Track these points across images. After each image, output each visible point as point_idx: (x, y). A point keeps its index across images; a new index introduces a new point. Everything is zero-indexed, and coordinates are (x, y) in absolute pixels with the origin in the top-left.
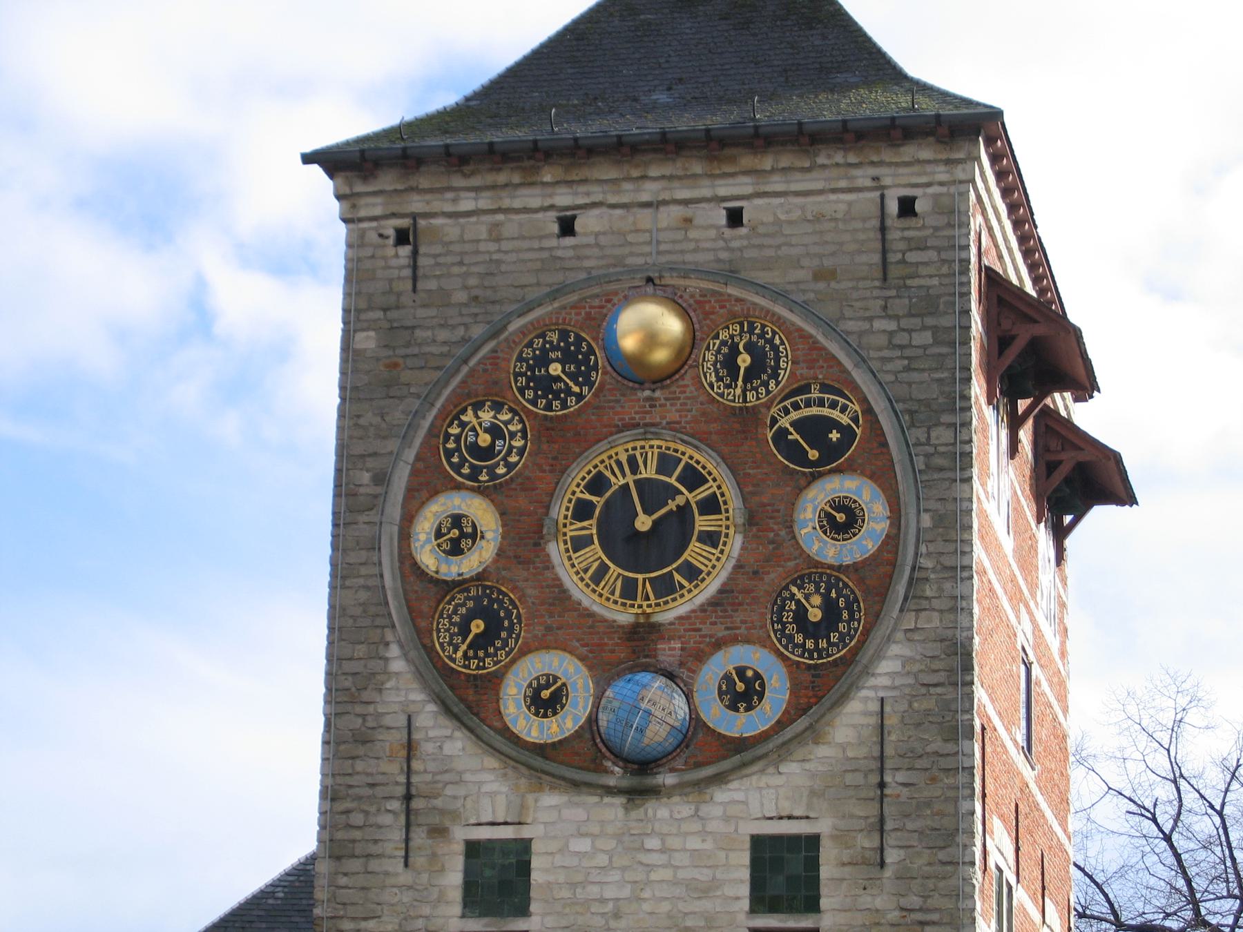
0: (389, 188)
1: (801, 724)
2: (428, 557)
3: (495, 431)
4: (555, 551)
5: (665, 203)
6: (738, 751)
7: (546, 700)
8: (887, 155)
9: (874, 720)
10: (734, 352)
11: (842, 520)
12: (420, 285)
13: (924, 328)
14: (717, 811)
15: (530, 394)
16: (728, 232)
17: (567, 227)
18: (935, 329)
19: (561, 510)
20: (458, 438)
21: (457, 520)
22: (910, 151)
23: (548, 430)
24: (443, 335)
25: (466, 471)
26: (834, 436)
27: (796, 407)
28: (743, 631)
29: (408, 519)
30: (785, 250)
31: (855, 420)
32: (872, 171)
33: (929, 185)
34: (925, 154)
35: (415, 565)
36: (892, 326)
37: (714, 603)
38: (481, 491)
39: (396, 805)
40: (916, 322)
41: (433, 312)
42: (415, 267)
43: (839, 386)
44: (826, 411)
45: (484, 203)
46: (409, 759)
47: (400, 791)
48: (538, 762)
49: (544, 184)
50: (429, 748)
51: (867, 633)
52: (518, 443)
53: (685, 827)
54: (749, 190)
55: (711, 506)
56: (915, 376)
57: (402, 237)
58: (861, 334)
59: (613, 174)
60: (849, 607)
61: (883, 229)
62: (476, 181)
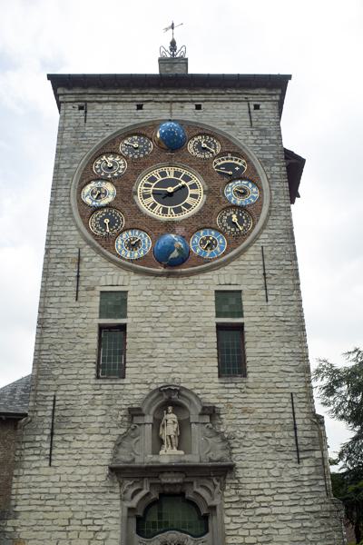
0: (78, 92)
2: (88, 200)
4: (139, 199)
7: (133, 246)
8: (251, 92)
10: (200, 143)
11: (242, 193)
17: (140, 107)
18: (270, 139)
20: (100, 165)
26: (237, 168)
28: (208, 225)
34: (264, 91)
35: (85, 204)
37: (195, 216)
40: (263, 138)
43: (238, 154)
44: (233, 161)
45: (110, 99)
46: (79, 263)
51: (254, 226)
52: (122, 167)
55: (194, 186)
57: (81, 108)
58: (245, 140)
60: (246, 219)
61: (250, 112)
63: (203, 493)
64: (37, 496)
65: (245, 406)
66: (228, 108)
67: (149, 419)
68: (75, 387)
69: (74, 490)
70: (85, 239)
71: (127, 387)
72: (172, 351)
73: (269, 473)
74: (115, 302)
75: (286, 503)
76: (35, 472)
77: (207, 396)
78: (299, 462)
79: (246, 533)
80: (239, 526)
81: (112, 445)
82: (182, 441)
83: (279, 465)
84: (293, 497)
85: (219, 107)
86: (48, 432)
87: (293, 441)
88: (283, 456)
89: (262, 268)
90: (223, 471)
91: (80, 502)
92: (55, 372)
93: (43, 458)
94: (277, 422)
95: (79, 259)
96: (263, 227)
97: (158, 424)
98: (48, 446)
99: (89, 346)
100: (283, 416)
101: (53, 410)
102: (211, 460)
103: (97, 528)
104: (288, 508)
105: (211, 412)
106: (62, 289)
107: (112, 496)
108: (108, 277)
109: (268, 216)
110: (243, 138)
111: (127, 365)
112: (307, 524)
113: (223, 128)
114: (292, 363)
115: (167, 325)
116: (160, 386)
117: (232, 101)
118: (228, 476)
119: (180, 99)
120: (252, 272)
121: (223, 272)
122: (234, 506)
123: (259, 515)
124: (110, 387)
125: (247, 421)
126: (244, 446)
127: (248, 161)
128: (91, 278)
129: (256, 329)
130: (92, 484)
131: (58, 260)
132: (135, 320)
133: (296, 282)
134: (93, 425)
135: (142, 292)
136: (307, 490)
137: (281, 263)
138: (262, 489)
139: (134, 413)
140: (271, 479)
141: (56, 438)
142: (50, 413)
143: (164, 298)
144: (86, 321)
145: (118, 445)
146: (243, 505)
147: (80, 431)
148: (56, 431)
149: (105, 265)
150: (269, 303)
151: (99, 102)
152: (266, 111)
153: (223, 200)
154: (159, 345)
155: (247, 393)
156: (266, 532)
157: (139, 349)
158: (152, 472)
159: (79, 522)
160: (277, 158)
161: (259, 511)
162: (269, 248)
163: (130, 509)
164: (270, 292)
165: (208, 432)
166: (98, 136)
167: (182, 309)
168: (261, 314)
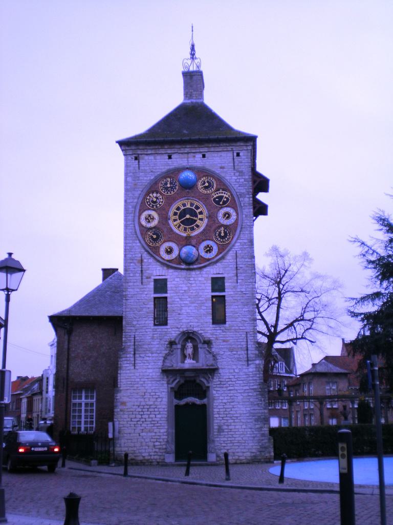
0: (133, 148)
1: (220, 256)
2: (144, 223)
3: (157, 198)
4: (171, 222)
5: (190, 153)
6: (208, 261)
8: (234, 144)
9: (235, 255)
12: (140, 168)
13: (243, 178)
14: (204, 273)
15: (163, 191)
16: (203, 159)
17: (170, 157)
18: (244, 179)
19: (171, 214)
21: (150, 216)
22: (238, 144)
23: (167, 198)
24: (145, 178)
25: (151, 206)
27: (217, 194)
28: (208, 238)
29: (140, 215)
30: (214, 163)
31: (229, 196)
32: (231, 147)
33: (242, 150)
34: (242, 144)
35: (141, 224)
36: (236, 178)
37: (202, 233)
38: (154, 210)
39: (140, 272)
41: (143, 174)
42: (139, 165)
43: (226, 189)
45: (153, 152)
47: (140, 269)
48: (168, 263)
49: (165, 148)
50: (145, 260)
51: (233, 238)
52: (161, 200)
53: (198, 276)
54: (206, 151)
55: (201, 213)
56: (240, 188)
57: (136, 159)
58: (230, 179)
59: (179, 147)
61: (234, 159)
62: (151, 148)
63: (205, 381)
64: (130, 383)
65: (224, 338)
66: (221, 156)
67: (179, 346)
68: (144, 331)
69: (147, 380)
70: (145, 249)
71: (169, 330)
72: (190, 311)
73: (234, 371)
74: (161, 285)
75: (242, 385)
76: (128, 372)
77: (207, 334)
78: (248, 366)
79: (223, 398)
80: (220, 395)
81: (163, 359)
82: (195, 356)
83: (239, 367)
84: (245, 382)
85: (216, 155)
86: (133, 353)
87: (246, 356)
88: (240, 363)
89: (235, 263)
90: (212, 371)
91: (149, 385)
92: (135, 323)
93: (131, 365)
94: (239, 346)
95: (142, 261)
96: (237, 239)
97: (183, 348)
98: (133, 359)
99: (150, 309)
100: (242, 343)
101: (135, 342)
102: (207, 366)
103: (157, 397)
104: (242, 387)
105: (208, 343)
106: (134, 278)
107: (164, 382)
108: (157, 271)
109: (240, 231)
110: (231, 178)
111: (168, 319)
112: (251, 394)
113: (218, 171)
114: (248, 317)
115: (187, 297)
116: (185, 329)
117: (224, 151)
118: (216, 372)
119: (193, 151)
120: (230, 266)
121: (215, 267)
122: (218, 386)
123: (229, 390)
124: (161, 330)
125: (225, 346)
126: (223, 359)
127: (232, 195)
128: (148, 272)
129: (231, 298)
130: (154, 377)
131: (131, 261)
132: (172, 295)
133: (253, 271)
134: (153, 349)
135: (175, 279)
136: (251, 378)
137: (246, 260)
138: (231, 379)
139: (172, 343)
140: (235, 374)
141: (137, 355)
142: (133, 343)
143: (186, 282)
144: (147, 296)
145: (165, 358)
146: (222, 386)
147: (148, 352)
148: (136, 352)
149: (155, 264)
150: (238, 284)
151: (147, 154)
152: (243, 157)
153: (216, 222)
154: (183, 308)
155: (225, 332)
156: (232, 398)
157: (173, 311)
158: (182, 372)
159: (149, 394)
160: (248, 192)
161: (229, 388)
162: (240, 252)
163: (171, 388)
164: (239, 278)
165: (207, 352)
166: (146, 179)
167: (194, 288)
168: (234, 290)
